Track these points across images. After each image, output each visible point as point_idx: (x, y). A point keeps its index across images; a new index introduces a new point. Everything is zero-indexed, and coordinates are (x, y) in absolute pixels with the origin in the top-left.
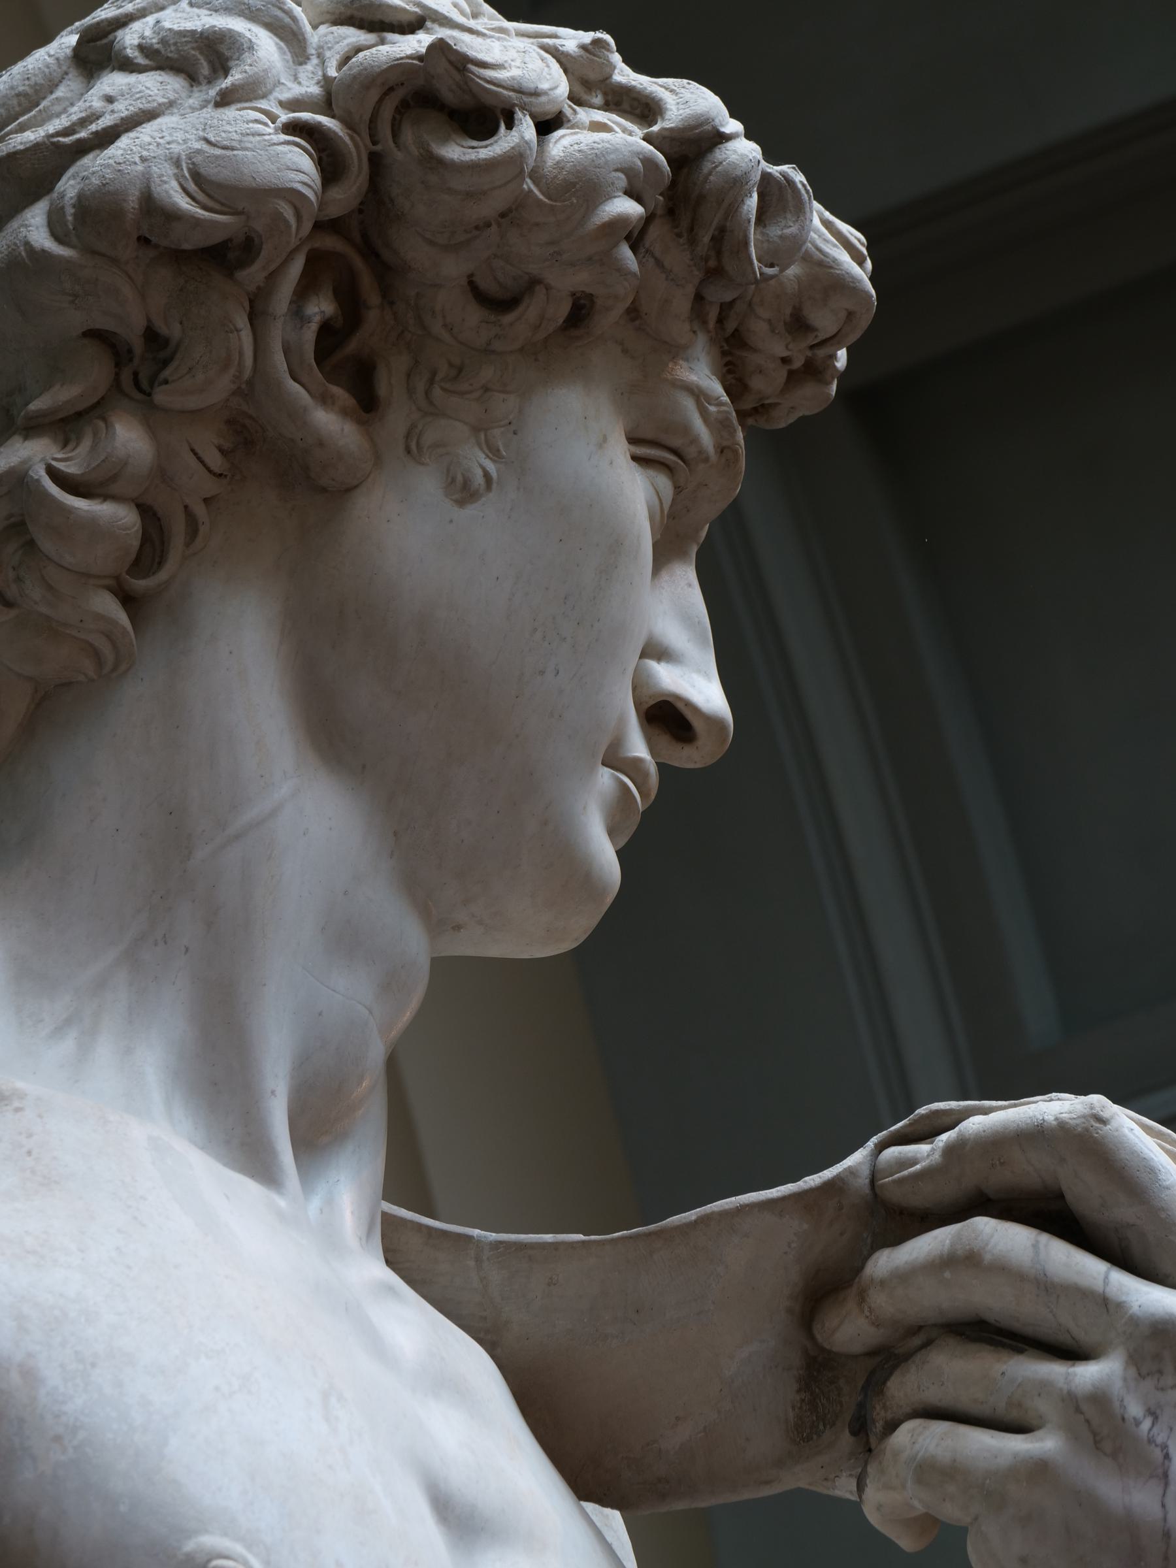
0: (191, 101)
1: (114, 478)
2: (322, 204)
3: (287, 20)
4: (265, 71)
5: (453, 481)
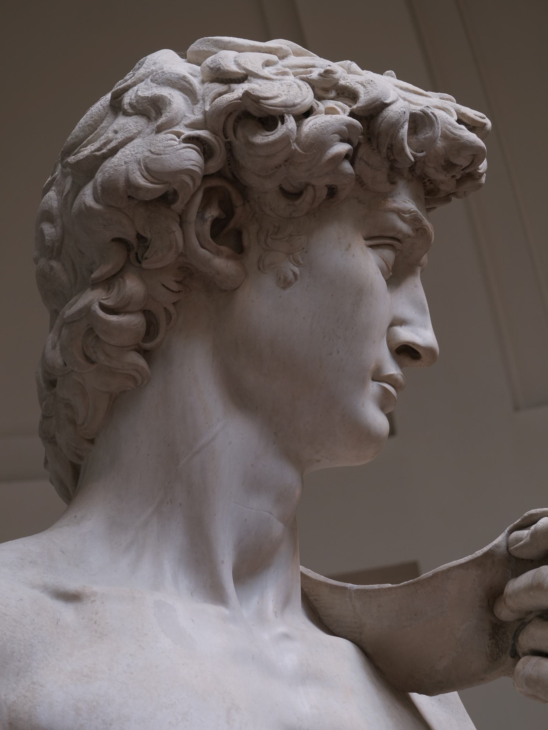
0: (148, 130)
2: (206, 169)
3: (188, 85)
4: (176, 114)
5: (280, 279)
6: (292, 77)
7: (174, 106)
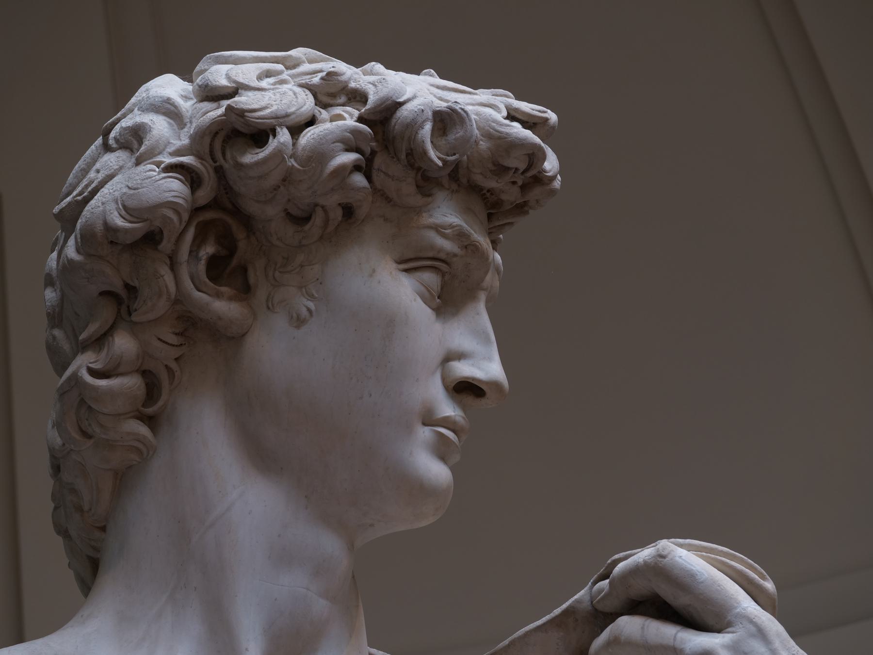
1: (119, 365)
3: (172, 108)
4: (157, 141)
7: (155, 132)
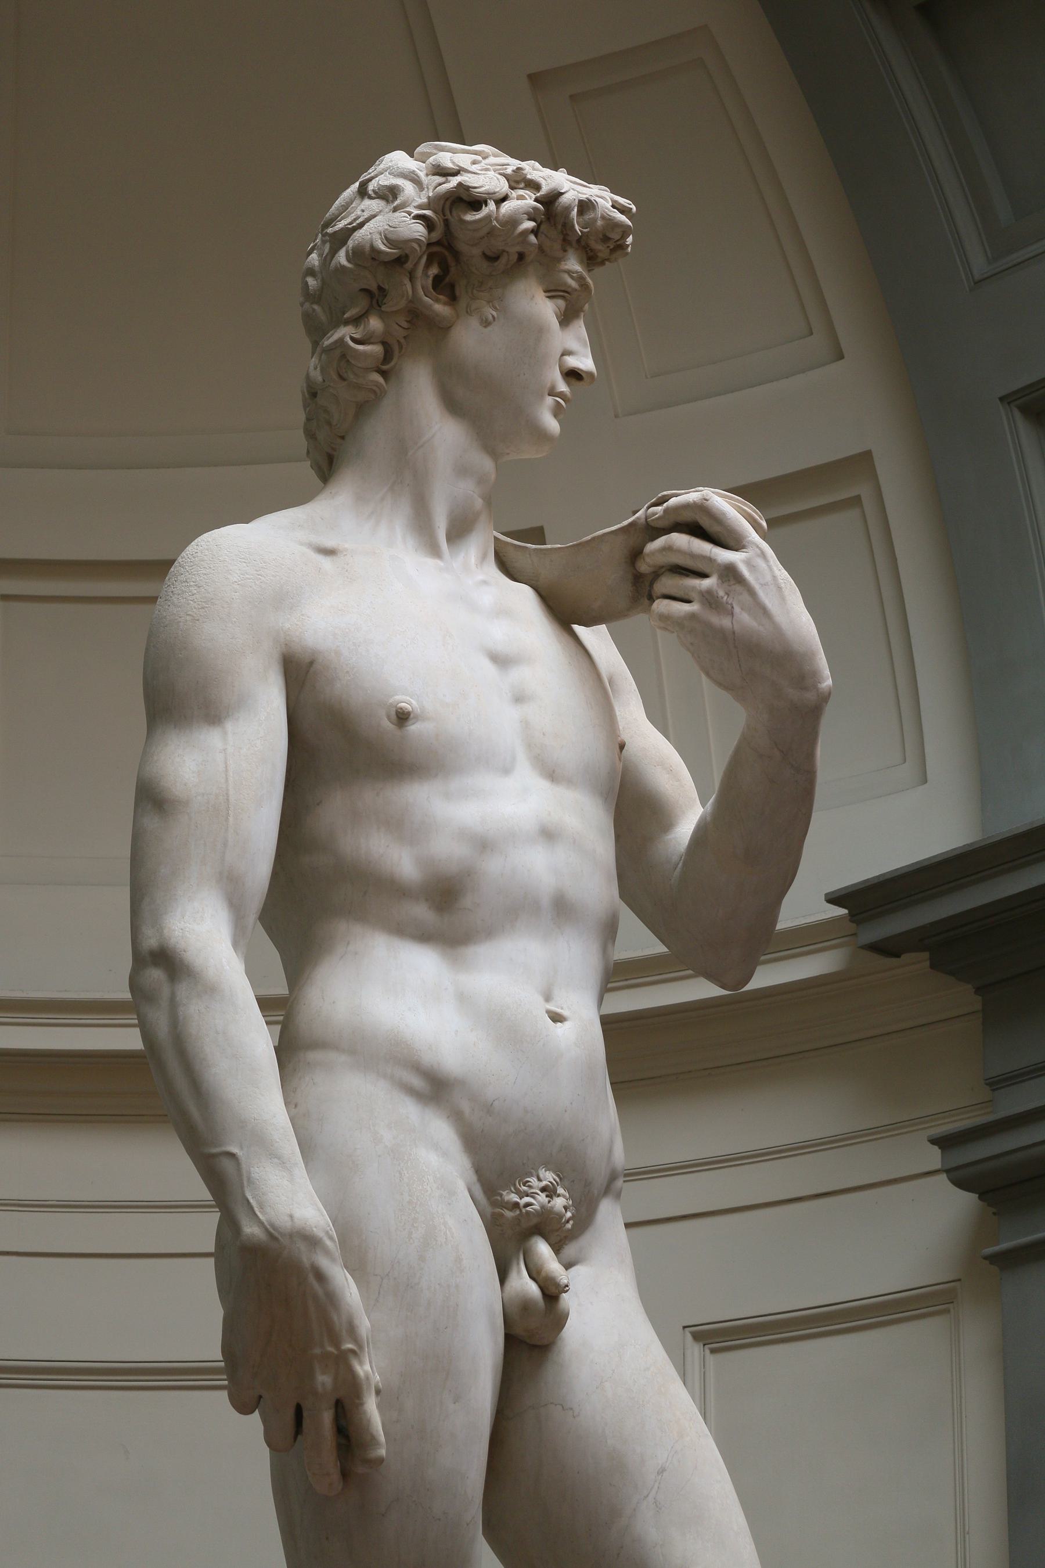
6: (492, 173)
7: (406, 192)
